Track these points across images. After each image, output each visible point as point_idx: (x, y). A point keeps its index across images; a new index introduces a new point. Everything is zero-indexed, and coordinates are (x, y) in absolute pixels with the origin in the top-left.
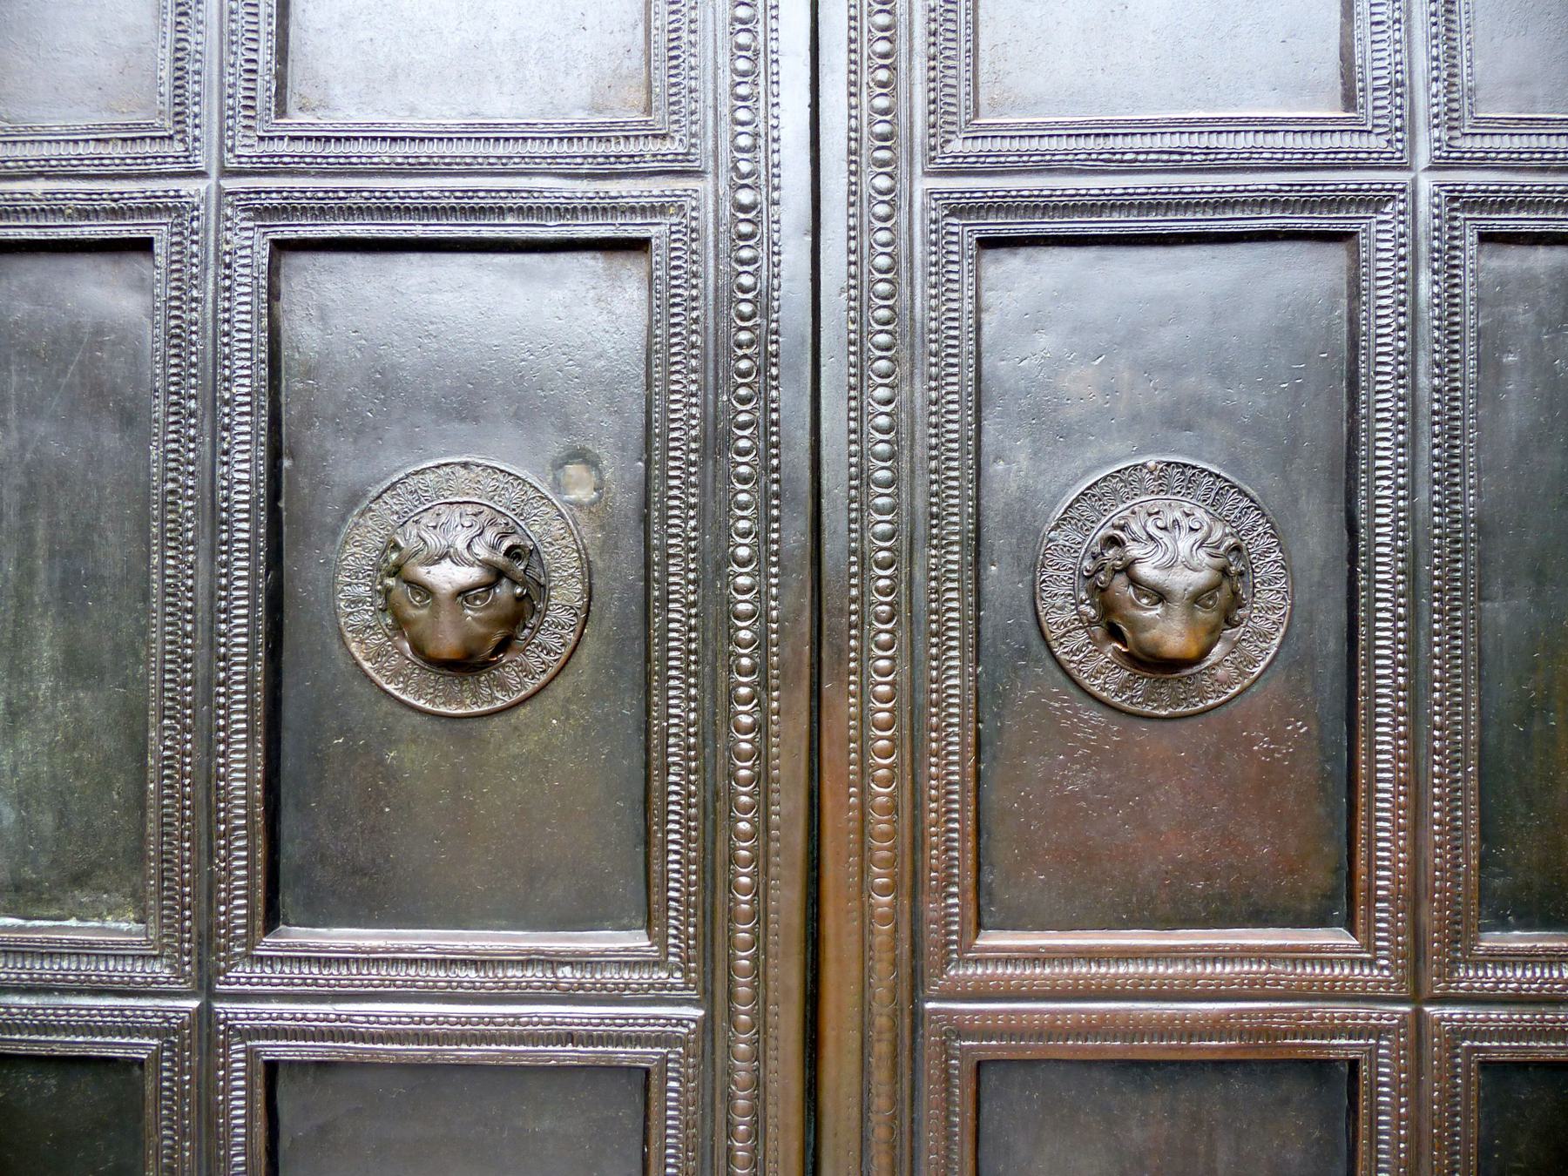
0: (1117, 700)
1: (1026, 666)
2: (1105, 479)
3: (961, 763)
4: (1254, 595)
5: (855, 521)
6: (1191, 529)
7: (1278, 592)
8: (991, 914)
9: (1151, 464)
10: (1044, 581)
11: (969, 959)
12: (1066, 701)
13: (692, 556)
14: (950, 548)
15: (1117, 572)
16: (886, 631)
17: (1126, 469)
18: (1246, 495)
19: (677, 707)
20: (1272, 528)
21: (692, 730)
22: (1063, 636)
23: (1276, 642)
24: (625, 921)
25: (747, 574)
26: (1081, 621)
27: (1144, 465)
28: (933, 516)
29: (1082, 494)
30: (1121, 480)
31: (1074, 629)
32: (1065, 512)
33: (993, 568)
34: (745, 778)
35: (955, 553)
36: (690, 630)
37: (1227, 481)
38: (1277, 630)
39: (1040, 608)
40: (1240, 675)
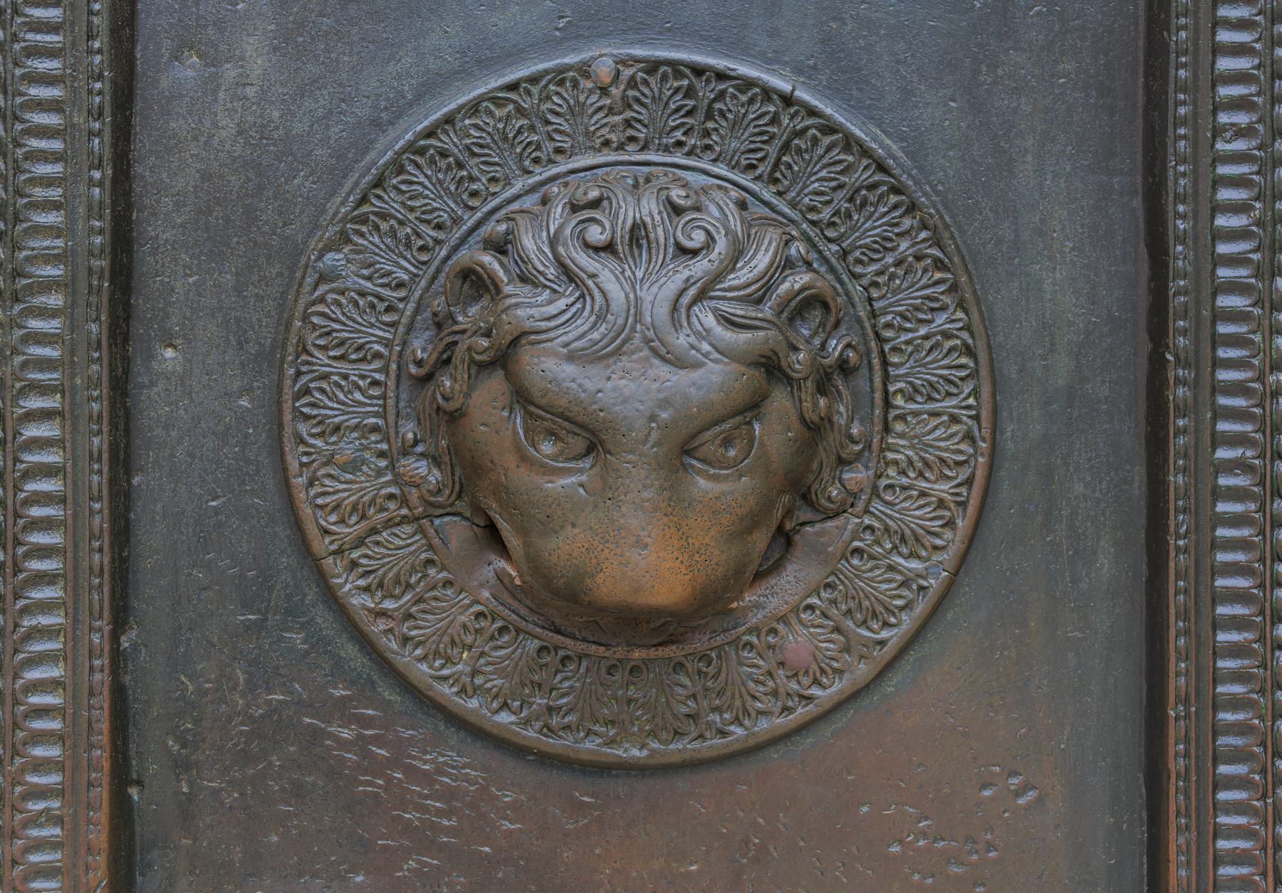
0: (505, 718)
1: (260, 626)
2: (474, 108)
4: (887, 429)
6: (683, 251)
7: (955, 419)
9: (604, 70)
10: (307, 391)
12: (365, 722)
15: (482, 366)
17: (534, 80)
18: (865, 152)
20: (938, 244)
22: (360, 542)
23: (947, 557)
26: (404, 502)
27: (584, 70)
29: (412, 148)
30: (520, 111)
31: (388, 524)
32: (364, 200)
33: (169, 353)
37: (812, 112)
38: (950, 524)
39: (293, 465)
40: (847, 649)
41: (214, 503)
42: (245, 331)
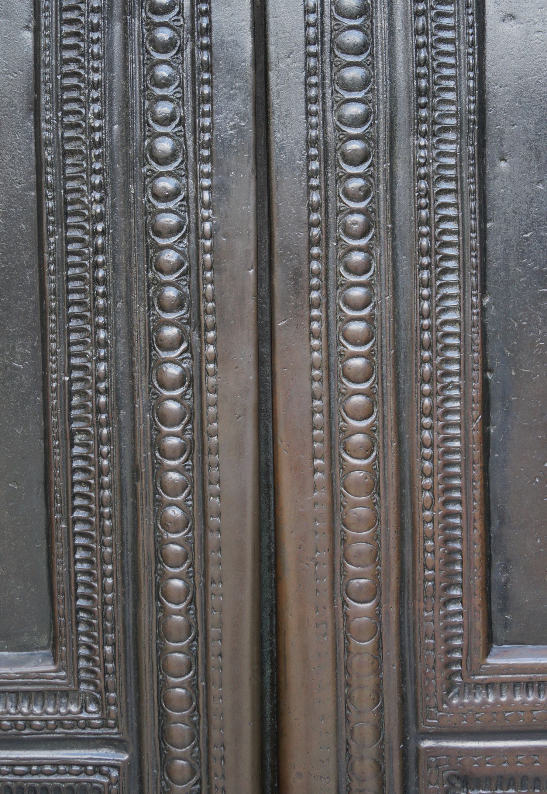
3: (463, 425)
5: (315, 101)
8: (506, 625)
11: (477, 684)
13: (97, 152)
14: (445, 136)
16: (360, 249)
19: (82, 355)
21: (102, 386)
24: (25, 639)
25: (170, 174)
28: (420, 92)
33: (503, 164)
34: (174, 448)
35: (451, 142)
36: (97, 252)
41: (526, 236)
42: (540, 152)
